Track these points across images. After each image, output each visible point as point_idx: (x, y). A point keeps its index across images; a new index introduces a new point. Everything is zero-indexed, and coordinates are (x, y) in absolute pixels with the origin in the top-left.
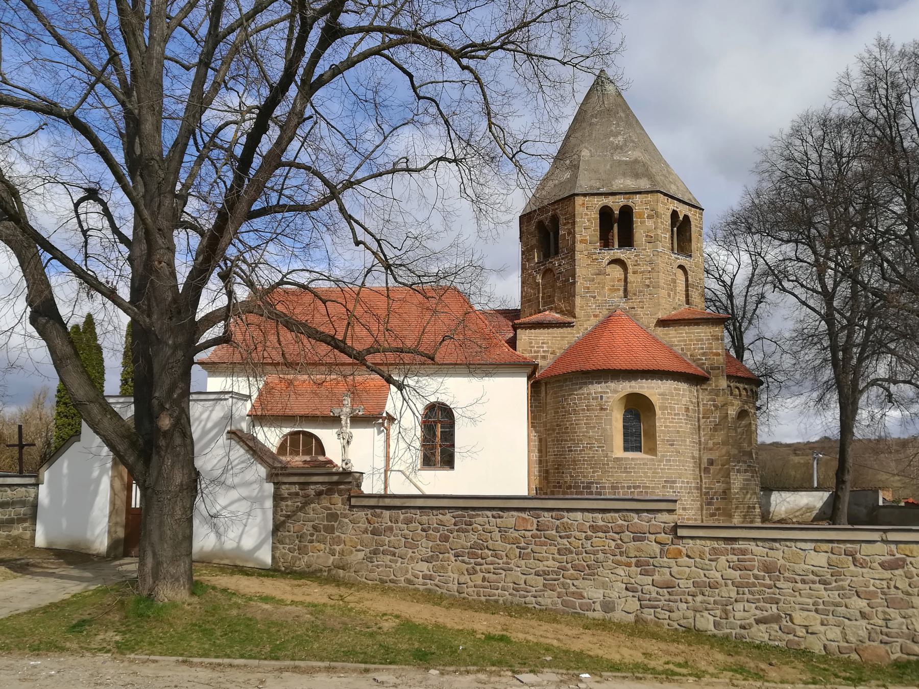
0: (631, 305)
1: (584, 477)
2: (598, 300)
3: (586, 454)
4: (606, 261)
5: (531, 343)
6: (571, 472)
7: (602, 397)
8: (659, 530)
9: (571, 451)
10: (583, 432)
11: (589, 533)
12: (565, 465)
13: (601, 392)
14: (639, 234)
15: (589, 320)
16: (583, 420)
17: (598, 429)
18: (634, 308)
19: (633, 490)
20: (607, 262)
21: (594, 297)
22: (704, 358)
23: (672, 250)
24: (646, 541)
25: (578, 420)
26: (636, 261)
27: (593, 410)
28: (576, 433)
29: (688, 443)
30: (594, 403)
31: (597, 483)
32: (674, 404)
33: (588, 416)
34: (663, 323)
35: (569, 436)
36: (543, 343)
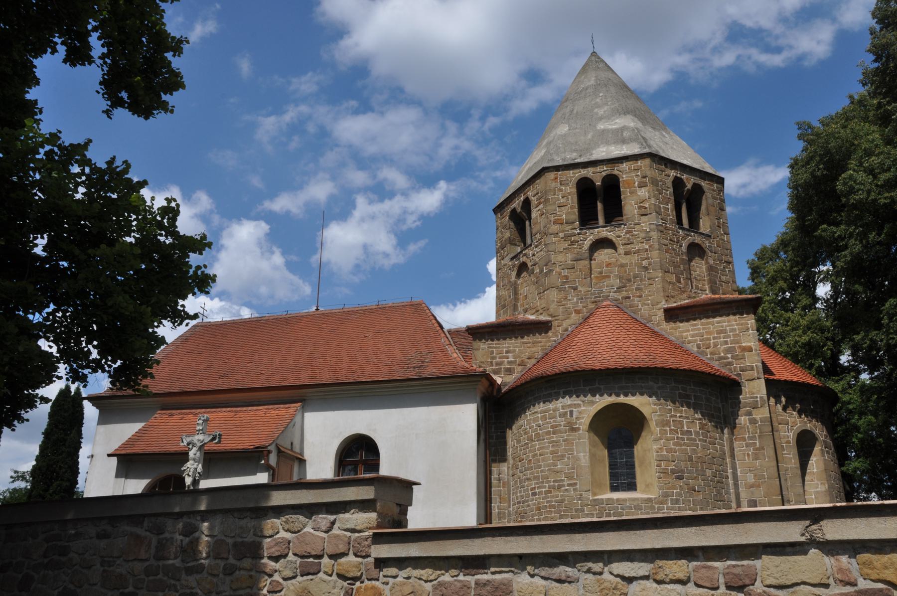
0: (624, 294)
2: (580, 291)
4: (587, 244)
5: (492, 353)
7: (571, 412)
8: (342, 548)
10: (548, 465)
11: (232, 561)
13: (570, 406)
14: (630, 206)
15: (568, 318)
17: (569, 458)
18: (629, 298)
20: (591, 242)
21: (575, 289)
22: (729, 356)
23: (679, 221)
24: (321, 575)
26: (629, 239)
28: (540, 467)
29: (709, 473)
32: (680, 417)
33: (553, 442)
34: (672, 315)
36: (507, 352)
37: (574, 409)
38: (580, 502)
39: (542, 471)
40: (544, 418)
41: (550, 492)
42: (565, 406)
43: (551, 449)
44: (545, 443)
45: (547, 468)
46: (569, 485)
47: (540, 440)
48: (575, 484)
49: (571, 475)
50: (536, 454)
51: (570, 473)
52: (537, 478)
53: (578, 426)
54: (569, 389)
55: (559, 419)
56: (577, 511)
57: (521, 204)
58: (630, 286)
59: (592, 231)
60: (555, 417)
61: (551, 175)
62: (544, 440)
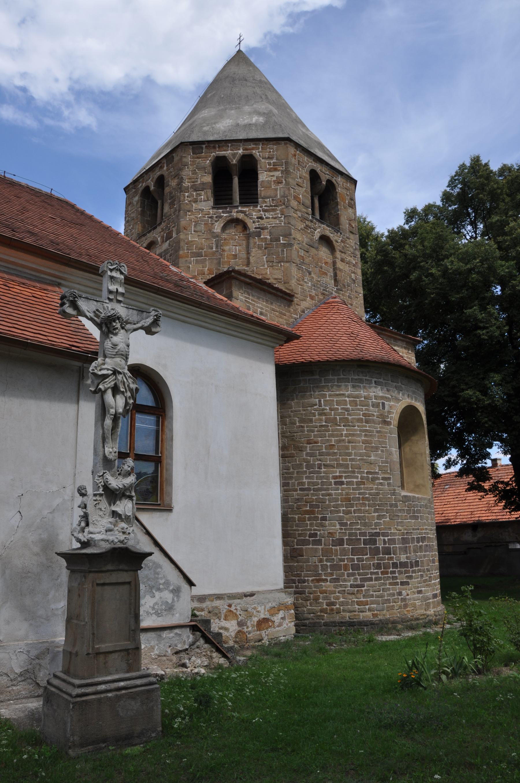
1: (365, 524)
3: (367, 489)
6: (341, 519)
9: (342, 483)
10: (361, 455)
12: (329, 506)
13: (382, 398)
16: (360, 436)
17: (382, 451)
19: (421, 544)
25: (353, 435)
27: (374, 422)
30: (375, 412)
31: (384, 535)
33: (366, 431)
35: (336, 460)
37: (386, 402)
38: (393, 497)
39: (352, 460)
42: (378, 396)
43: (363, 438)
44: (356, 430)
45: (359, 458)
46: (383, 479)
47: (349, 426)
48: (389, 479)
49: (386, 469)
50: (344, 440)
51: (384, 466)
52: (347, 466)
53: (389, 420)
54: (380, 380)
55: (371, 408)
56: (391, 505)
57: (238, 157)
58: (345, 292)
59: (320, 225)
60: (368, 405)
61: (292, 150)
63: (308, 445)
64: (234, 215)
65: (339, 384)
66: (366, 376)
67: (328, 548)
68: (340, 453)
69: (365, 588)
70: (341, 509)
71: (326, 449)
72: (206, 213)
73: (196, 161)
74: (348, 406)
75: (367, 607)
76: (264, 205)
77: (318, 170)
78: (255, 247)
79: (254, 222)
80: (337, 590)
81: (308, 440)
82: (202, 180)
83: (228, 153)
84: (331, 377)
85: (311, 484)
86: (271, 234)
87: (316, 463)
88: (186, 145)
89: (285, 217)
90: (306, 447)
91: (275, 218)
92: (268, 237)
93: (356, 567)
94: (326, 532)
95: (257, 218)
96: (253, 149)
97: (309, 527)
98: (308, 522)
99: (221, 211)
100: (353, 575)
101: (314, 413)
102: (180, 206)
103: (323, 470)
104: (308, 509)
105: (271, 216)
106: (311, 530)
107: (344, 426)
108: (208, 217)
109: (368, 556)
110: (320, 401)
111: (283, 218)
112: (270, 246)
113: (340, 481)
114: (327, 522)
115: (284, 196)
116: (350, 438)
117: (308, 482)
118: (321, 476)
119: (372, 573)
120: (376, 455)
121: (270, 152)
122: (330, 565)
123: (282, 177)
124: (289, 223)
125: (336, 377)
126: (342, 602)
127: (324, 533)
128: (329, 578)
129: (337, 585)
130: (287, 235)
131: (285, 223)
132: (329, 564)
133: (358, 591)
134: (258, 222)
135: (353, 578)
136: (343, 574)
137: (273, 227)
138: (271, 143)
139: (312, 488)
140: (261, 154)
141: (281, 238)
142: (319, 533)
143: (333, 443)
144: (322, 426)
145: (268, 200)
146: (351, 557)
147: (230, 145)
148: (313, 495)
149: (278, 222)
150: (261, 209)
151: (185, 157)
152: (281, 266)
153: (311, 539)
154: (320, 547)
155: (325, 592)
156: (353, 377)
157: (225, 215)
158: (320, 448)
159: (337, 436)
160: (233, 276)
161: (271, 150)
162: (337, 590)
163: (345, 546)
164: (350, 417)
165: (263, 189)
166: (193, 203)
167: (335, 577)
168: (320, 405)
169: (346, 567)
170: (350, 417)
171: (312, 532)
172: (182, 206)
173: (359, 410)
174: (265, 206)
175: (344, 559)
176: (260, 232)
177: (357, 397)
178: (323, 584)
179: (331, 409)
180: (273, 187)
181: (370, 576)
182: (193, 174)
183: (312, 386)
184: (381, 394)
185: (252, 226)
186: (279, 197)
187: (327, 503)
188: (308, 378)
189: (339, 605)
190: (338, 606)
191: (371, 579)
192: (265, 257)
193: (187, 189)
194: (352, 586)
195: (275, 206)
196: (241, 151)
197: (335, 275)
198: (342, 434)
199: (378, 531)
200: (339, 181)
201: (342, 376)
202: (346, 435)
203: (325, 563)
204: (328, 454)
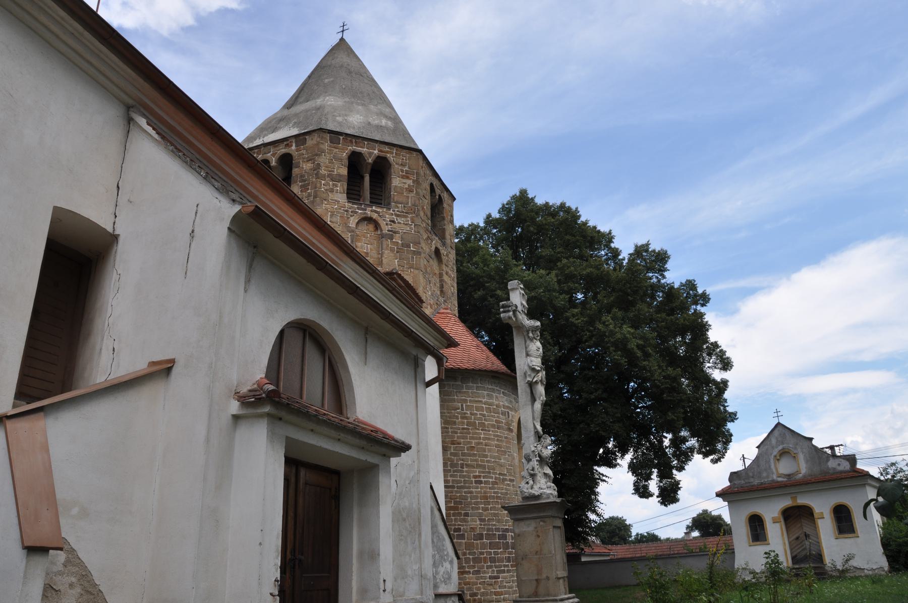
1: (499, 521)
3: (499, 488)
6: (481, 514)
9: (481, 482)
10: (494, 457)
12: (470, 503)
13: (508, 407)
16: (493, 440)
17: (509, 455)
25: (489, 439)
28: (486, 456)
30: (503, 419)
33: (497, 436)
39: (488, 461)
40: (489, 410)
41: (496, 483)
44: (490, 434)
45: (493, 460)
46: (511, 480)
47: (485, 430)
50: (482, 443)
52: (484, 467)
55: (501, 416)
60: (498, 413)
61: (421, 162)
62: (489, 431)
63: (452, 446)
64: (368, 213)
65: (478, 391)
66: (497, 387)
67: (470, 542)
68: (479, 454)
69: (500, 579)
70: (481, 506)
71: (467, 450)
72: (342, 205)
73: (333, 150)
74: (485, 413)
75: (502, 597)
76: (396, 210)
77: (434, 184)
78: (387, 249)
79: (387, 224)
80: (479, 581)
81: (452, 441)
82: (338, 171)
83: (364, 150)
84: (471, 384)
85: (455, 482)
86: (402, 239)
87: (460, 462)
88: (325, 132)
89: (415, 225)
90: (451, 447)
91: (406, 224)
92: (400, 242)
93: (493, 560)
94: (468, 527)
95: (390, 221)
96: (387, 152)
97: (453, 523)
98: (453, 518)
99: (356, 206)
100: (491, 567)
101: (457, 417)
102: (316, 192)
103: (465, 469)
104: (452, 505)
105: (402, 222)
106: (455, 525)
107: (481, 430)
108: (343, 210)
109: (502, 550)
110: (462, 405)
111: (413, 226)
112: (402, 251)
113: (479, 480)
114: (469, 518)
115: (414, 205)
116: (486, 441)
117: (452, 480)
118: (463, 475)
119: (505, 566)
120: (505, 459)
121: (403, 159)
122: (472, 558)
123: (413, 186)
124: (418, 232)
125: (475, 385)
126: (483, 593)
127: (467, 528)
128: (471, 570)
129: (478, 577)
130: (417, 243)
131: (415, 231)
132: (471, 557)
133: (495, 582)
134: (391, 225)
135: (491, 570)
136: (483, 566)
137: (405, 233)
138: (405, 151)
139: (456, 485)
140: (395, 159)
141: (411, 245)
142: (462, 528)
143: (473, 445)
144: (463, 429)
145: (400, 205)
146: (489, 550)
147: (366, 143)
148: (456, 492)
149: (408, 229)
150: (393, 213)
151: (322, 143)
152: (411, 272)
153: (456, 533)
154: (463, 541)
155: (468, 583)
156: (488, 386)
157: (360, 211)
158: (462, 449)
159: (476, 438)
160: (395, 277)
161: (404, 158)
162: (479, 581)
163: (484, 540)
164: (486, 423)
165: (396, 194)
166: (329, 193)
167: (476, 569)
168: (462, 410)
169: (485, 560)
170: (486, 423)
171: (457, 527)
172: (318, 193)
173: (492, 416)
174: (398, 211)
175: (484, 552)
176: (392, 235)
177: (491, 404)
178: (467, 576)
179: (471, 414)
180: (405, 194)
181: (503, 568)
182: (330, 163)
183: (455, 391)
184: (507, 404)
185: (385, 229)
186: (410, 205)
187: (469, 500)
188: (452, 383)
189: (481, 596)
190: (479, 597)
191: (504, 571)
192: (396, 261)
193: (323, 177)
194: (490, 577)
195: (406, 213)
196: (376, 152)
197: (442, 287)
198: (480, 437)
199: (507, 527)
200: (445, 195)
201: (480, 385)
202: (485, 439)
203: (468, 556)
204: (470, 455)
